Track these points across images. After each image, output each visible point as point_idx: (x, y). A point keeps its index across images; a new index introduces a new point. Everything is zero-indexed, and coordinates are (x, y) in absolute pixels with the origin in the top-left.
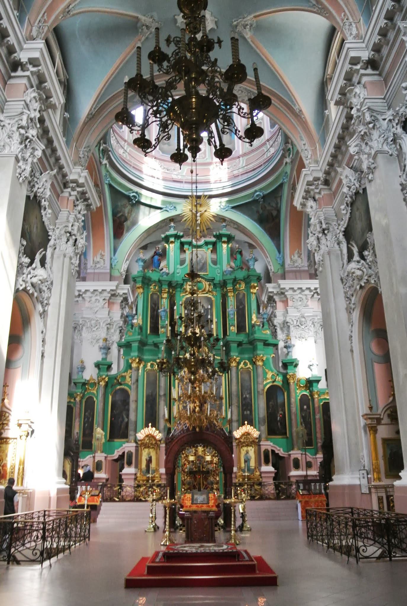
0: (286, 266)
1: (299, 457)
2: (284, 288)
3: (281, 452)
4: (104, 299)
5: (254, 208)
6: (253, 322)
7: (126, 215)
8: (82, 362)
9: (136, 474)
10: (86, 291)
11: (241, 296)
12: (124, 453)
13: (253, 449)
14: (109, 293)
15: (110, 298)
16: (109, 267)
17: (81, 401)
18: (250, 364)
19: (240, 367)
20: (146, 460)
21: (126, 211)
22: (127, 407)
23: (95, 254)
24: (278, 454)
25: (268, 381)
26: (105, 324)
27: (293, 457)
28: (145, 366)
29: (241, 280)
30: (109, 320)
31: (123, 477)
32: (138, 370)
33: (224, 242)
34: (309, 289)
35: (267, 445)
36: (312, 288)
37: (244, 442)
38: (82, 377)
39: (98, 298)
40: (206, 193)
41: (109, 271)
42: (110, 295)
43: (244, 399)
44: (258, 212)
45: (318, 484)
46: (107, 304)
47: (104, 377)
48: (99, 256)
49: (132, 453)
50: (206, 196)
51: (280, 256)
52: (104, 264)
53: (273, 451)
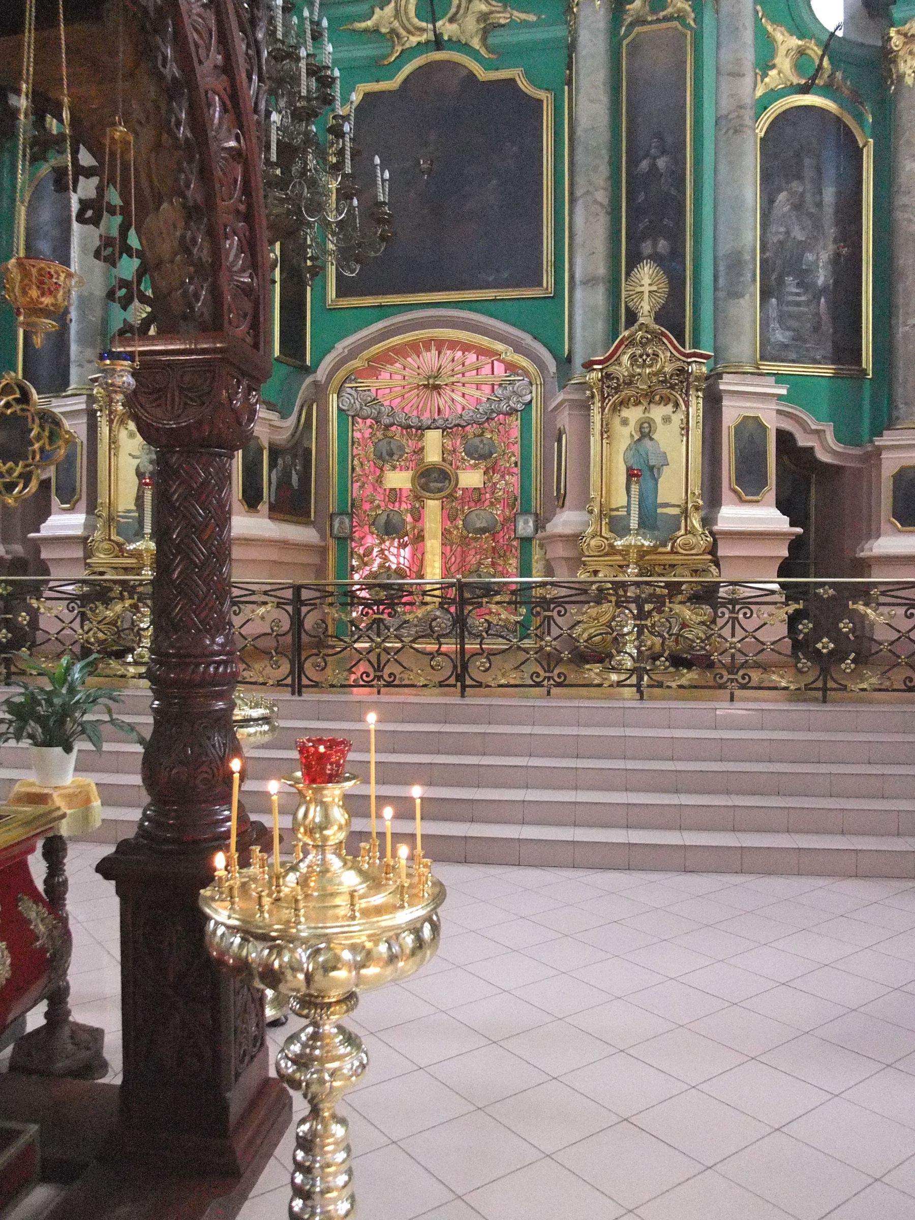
24: (811, 449)
25: (773, 79)
31: (44, 555)
35: (757, 399)
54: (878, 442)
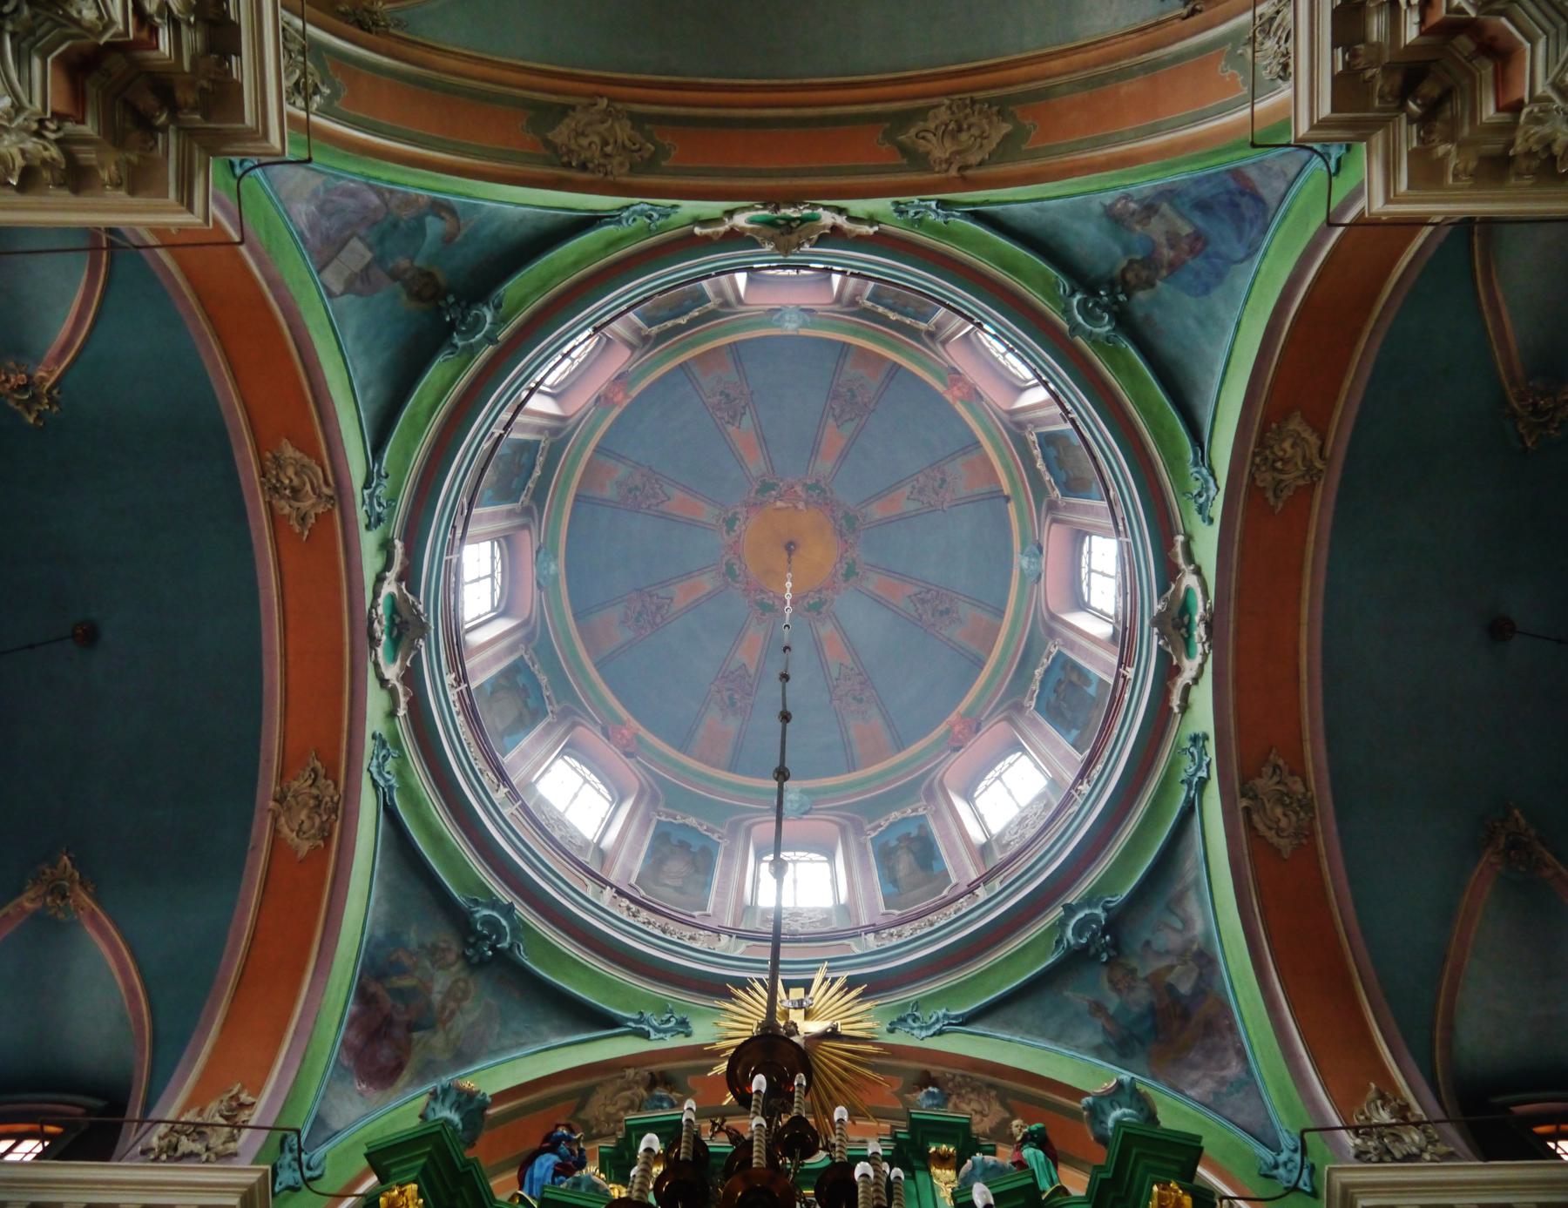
5: (1076, 996)
7: (436, 998)
33: (943, 1160)
44: (1098, 1008)
51: (1283, 1157)
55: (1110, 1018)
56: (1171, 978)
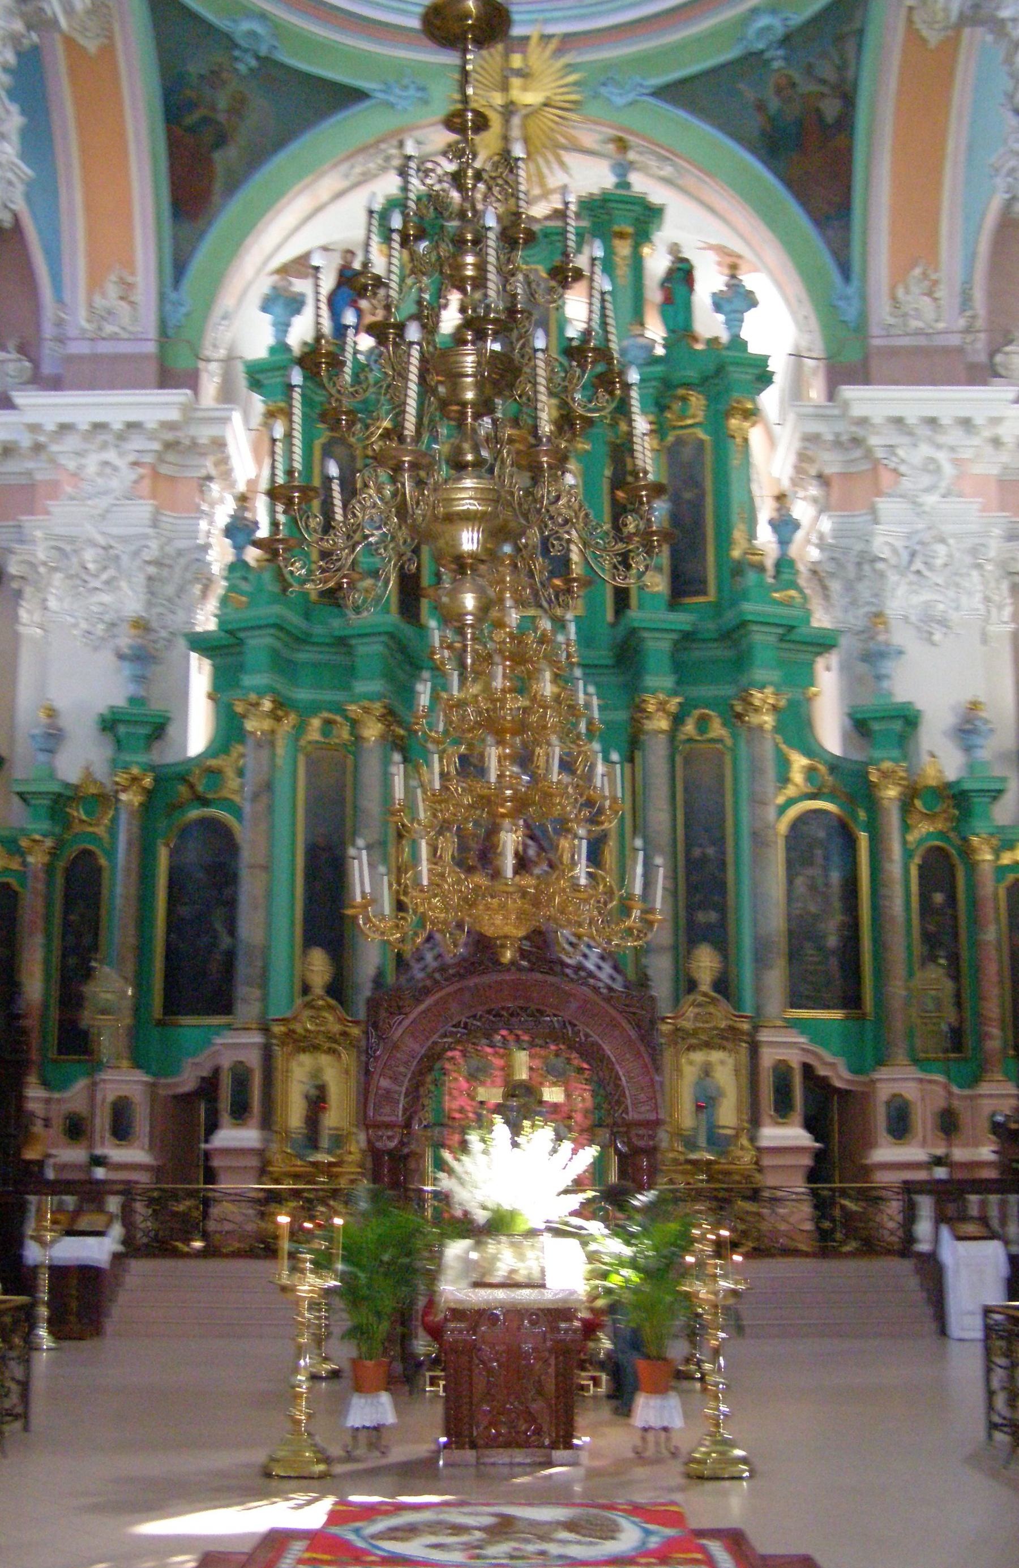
0: (875, 330)
1: (910, 1091)
2: (863, 422)
3: (839, 1074)
4: (135, 464)
6: (736, 553)
7: (221, 117)
8: (52, 713)
9: (260, 1153)
10: (65, 428)
11: (687, 453)
12: (217, 1071)
13: (730, 1061)
14: (152, 436)
15: (160, 457)
16: (152, 333)
17: (49, 869)
18: (724, 725)
19: (682, 737)
20: (307, 1097)
21: (222, 104)
22: (227, 891)
23: (95, 283)
26: (138, 562)
27: (884, 1092)
28: (301, 728)
29: (688, 386)
30: (154, 544)
32: (272, 744)
34: (966, 423)
36: (979, 420)
37: (695, 1033)
38: (52, 776)
39: (111, 455)
40: (550, 30)
41: (151, 348)
42: (156, 446)
43: (693, 865)
45: (994, 1198)
46: (147, 483)
47: (135, 771)
48: (112, 290)
49: (249, 1071)
50: (550, 37)
51: (851, 290)
52: (135, 320)
53: (807, 1069)
54: (876, 1076)
55: (772, 120)
56: (821, 105)
